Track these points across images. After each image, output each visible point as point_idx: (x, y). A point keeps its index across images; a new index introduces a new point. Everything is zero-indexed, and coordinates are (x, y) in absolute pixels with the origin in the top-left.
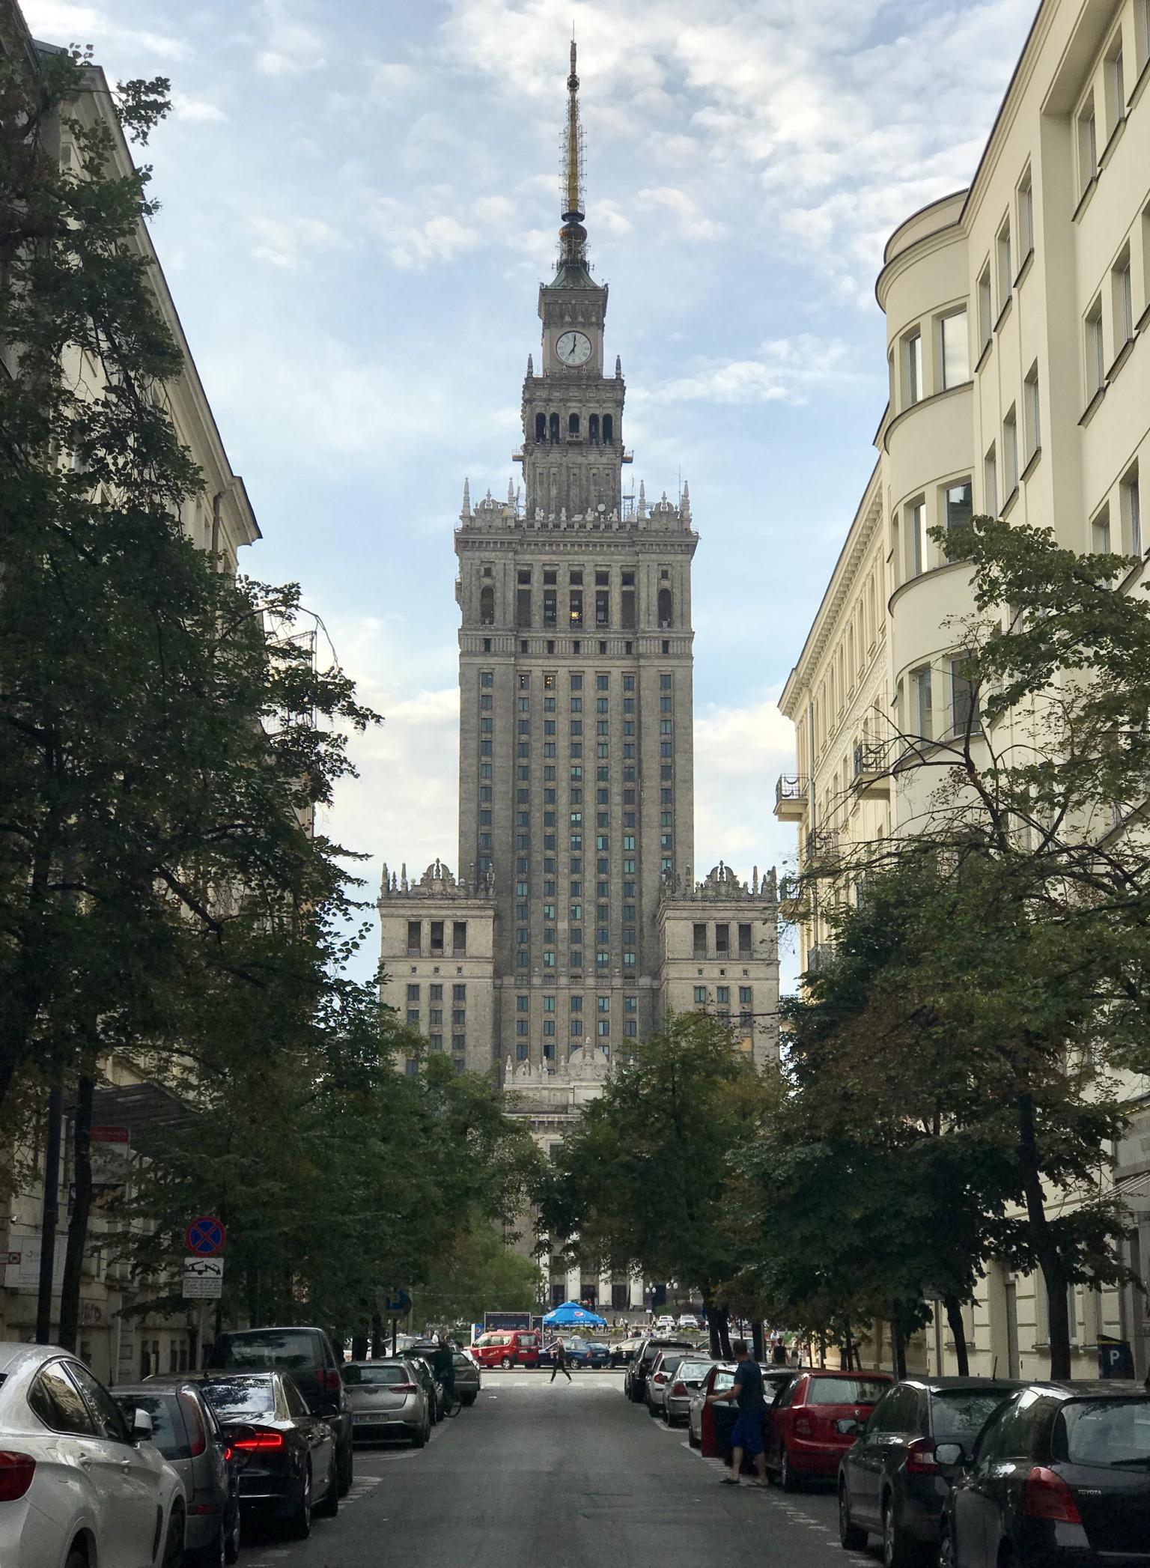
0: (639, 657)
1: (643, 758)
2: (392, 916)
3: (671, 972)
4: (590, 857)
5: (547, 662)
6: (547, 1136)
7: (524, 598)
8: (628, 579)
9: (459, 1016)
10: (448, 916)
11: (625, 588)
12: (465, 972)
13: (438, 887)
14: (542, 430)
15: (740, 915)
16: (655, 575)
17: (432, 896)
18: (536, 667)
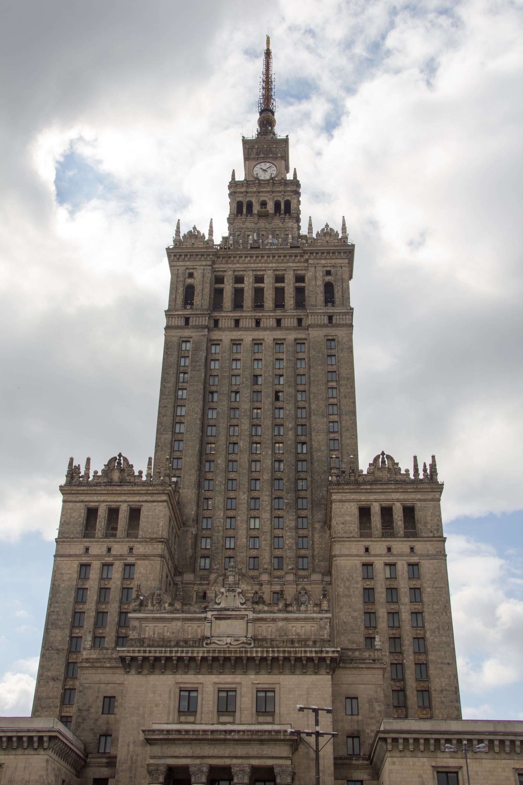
3: (337, 549)
8: (300, 279)
11: (298, 285)
13: (116, 476)
16: (320, 274)
17: (110, 483)
18: (226, 337)
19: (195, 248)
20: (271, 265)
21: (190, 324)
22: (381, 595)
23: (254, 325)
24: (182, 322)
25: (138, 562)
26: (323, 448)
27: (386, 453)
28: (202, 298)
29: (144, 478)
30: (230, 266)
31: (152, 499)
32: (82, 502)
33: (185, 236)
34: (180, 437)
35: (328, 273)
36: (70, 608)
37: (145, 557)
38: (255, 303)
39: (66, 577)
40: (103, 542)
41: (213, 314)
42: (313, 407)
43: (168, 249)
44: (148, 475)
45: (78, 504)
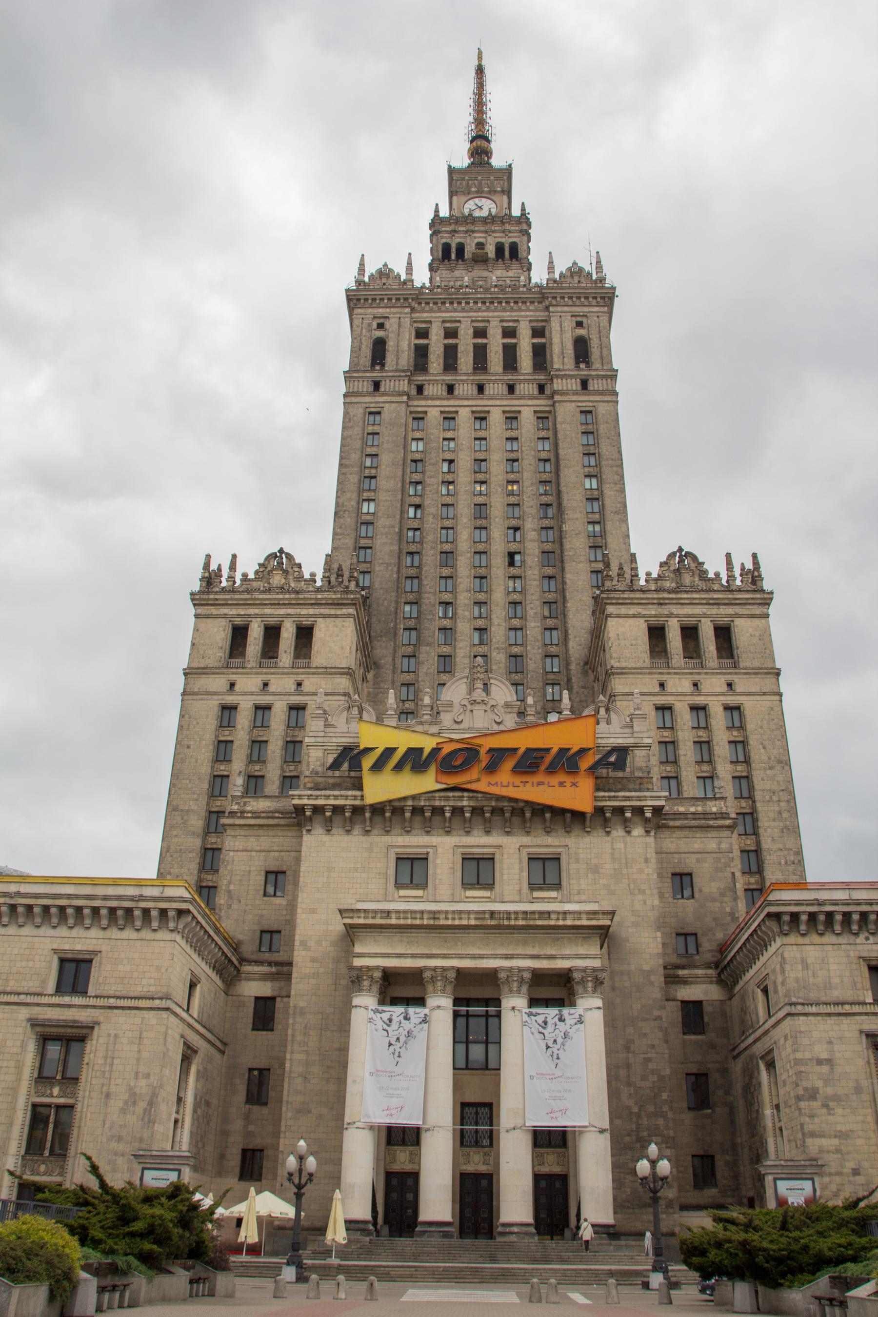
1: (563, 489)
2: (208, 617)
4: (499, 596)
5: (445, 403)
6: (387, 839)
7: (421, 353)
8: (538, 332)
9: (293, 746)
10: (288, 616)
11: (535, 341)
12: (307, 687)
13: (277, 579)
14: (446, 255)
15: (714, 610)
16: (569, 324)
17: (269, 590)
19: (387, 289)
22: (687, 752)
23: (475, 392)
24: (368, 387)
27: (686, 549)
29: (319, 583)
33: (371, 276)
35: (579, 324)
36: (205, 769)
38: (474, 364)
40: (258, 673)
41: (415, 378)
43: (347, 290)
44: (327, 579)
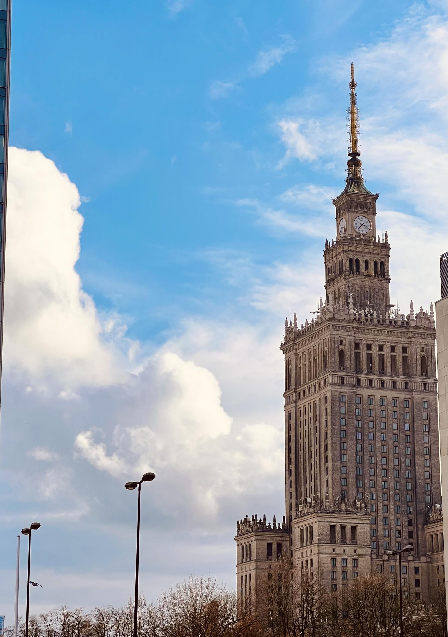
0: (412, 391)
8: (405, 350)
16: (419, 350)
20: (388, 338)
21: (345, 382)
24: (340, 381)
25: (359, 558)
26: (422, 477)
28: (349, 363)
30: (364, 336)
31: (362, 522)
32: (328, 522)
34: (345, 464)
37: (362, 556)
39: (326, 565)
42: (416, 449)
45: (326, 523)
